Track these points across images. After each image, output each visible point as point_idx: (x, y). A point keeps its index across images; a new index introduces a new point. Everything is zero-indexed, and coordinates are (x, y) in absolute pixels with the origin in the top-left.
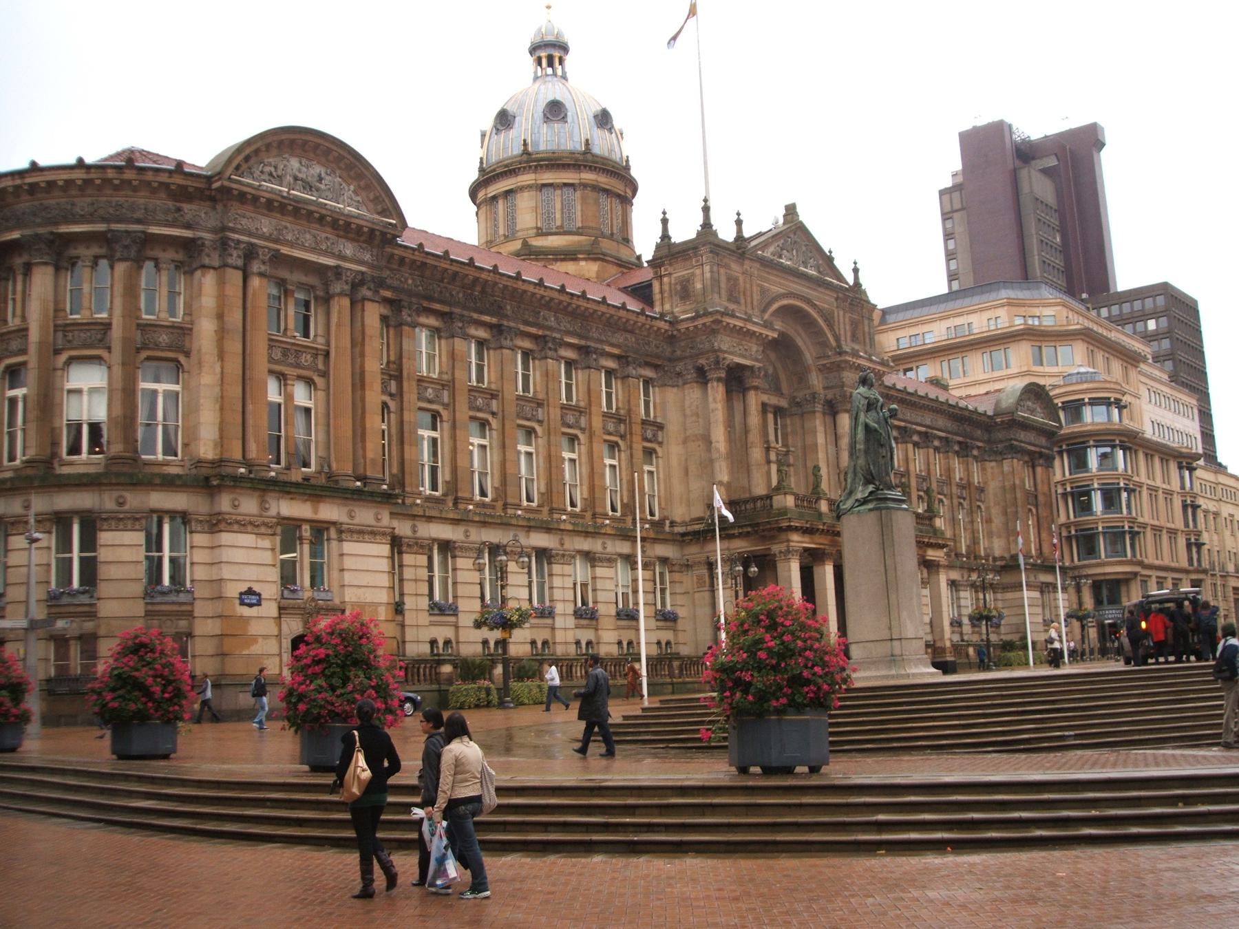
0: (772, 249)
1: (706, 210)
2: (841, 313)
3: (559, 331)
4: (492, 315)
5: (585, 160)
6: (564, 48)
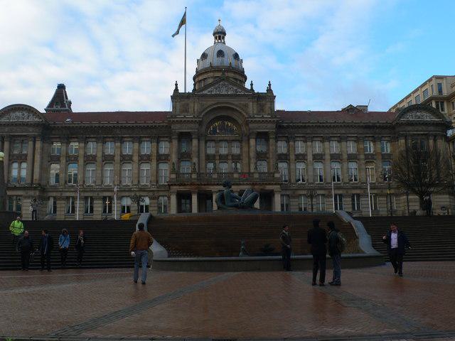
1: (176, 85)
2: (251, 103)
5: (230, 69)
6: (225, 34)
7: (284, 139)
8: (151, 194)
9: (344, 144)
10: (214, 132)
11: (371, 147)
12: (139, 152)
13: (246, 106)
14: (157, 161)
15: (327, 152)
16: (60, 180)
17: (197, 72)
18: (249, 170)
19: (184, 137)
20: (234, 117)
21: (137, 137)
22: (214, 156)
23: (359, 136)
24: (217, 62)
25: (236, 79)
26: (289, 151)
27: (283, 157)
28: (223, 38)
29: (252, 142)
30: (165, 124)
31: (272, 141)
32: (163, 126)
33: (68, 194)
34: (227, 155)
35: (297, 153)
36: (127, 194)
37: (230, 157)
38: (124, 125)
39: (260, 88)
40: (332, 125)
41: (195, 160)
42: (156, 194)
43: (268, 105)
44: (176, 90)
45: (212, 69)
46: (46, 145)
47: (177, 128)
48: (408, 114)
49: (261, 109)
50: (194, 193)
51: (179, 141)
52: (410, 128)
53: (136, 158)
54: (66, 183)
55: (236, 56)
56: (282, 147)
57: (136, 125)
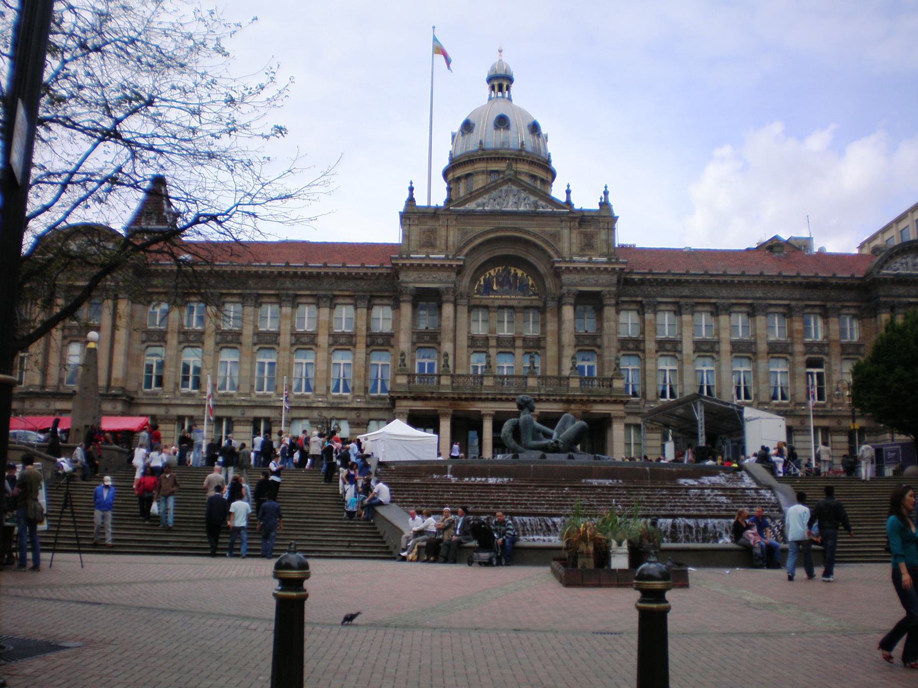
0: (480, 201)
1: (411, 189)
2: (566, 232)
3: (293, 289)
4: (238, 289)
7: (633, 306)
8: (353, 415)
9: (761, 320)
10: (488, 289)
11: (817, 330)
12: (330, 327)
13: (556, 236)
14: (368, 346)
15: (725, 335)
16: (165, 381)
17: (452, 159)
18: (560, 370)
19: (427, 299)
20: (531, 259)
21: (325, 296)
22: (487, 339)
23: (793, 303)
24: (493, 139)
25: (534, 177)
26: (643, 332)
27: (631, 346)
28: (508, 88)
29: (568, 312)
30: (384, 271)
31: (609, 312)
32: (381, 274)
33: (182, 411)
34: (514, 339)
35: (660, 337)
36: (303, 414)
37: (519, 343)
38: (299, 271)
39: (586, 201)
40: (736, 279)
41: (447, 347)
42: (364, 416)
43: (603, 235)
44: (411, 200)
45: (484, 155)
46: (139, 307)
47: (411, 281)
48: (899, 260)
49: (588, 245)
50: (445, 415)
51: (415, 307)
52: (901, 290)
53: (323, 340)
54: (177, 384)
55: (535, 128)
56: (627, 323)
57: (327, 270)
